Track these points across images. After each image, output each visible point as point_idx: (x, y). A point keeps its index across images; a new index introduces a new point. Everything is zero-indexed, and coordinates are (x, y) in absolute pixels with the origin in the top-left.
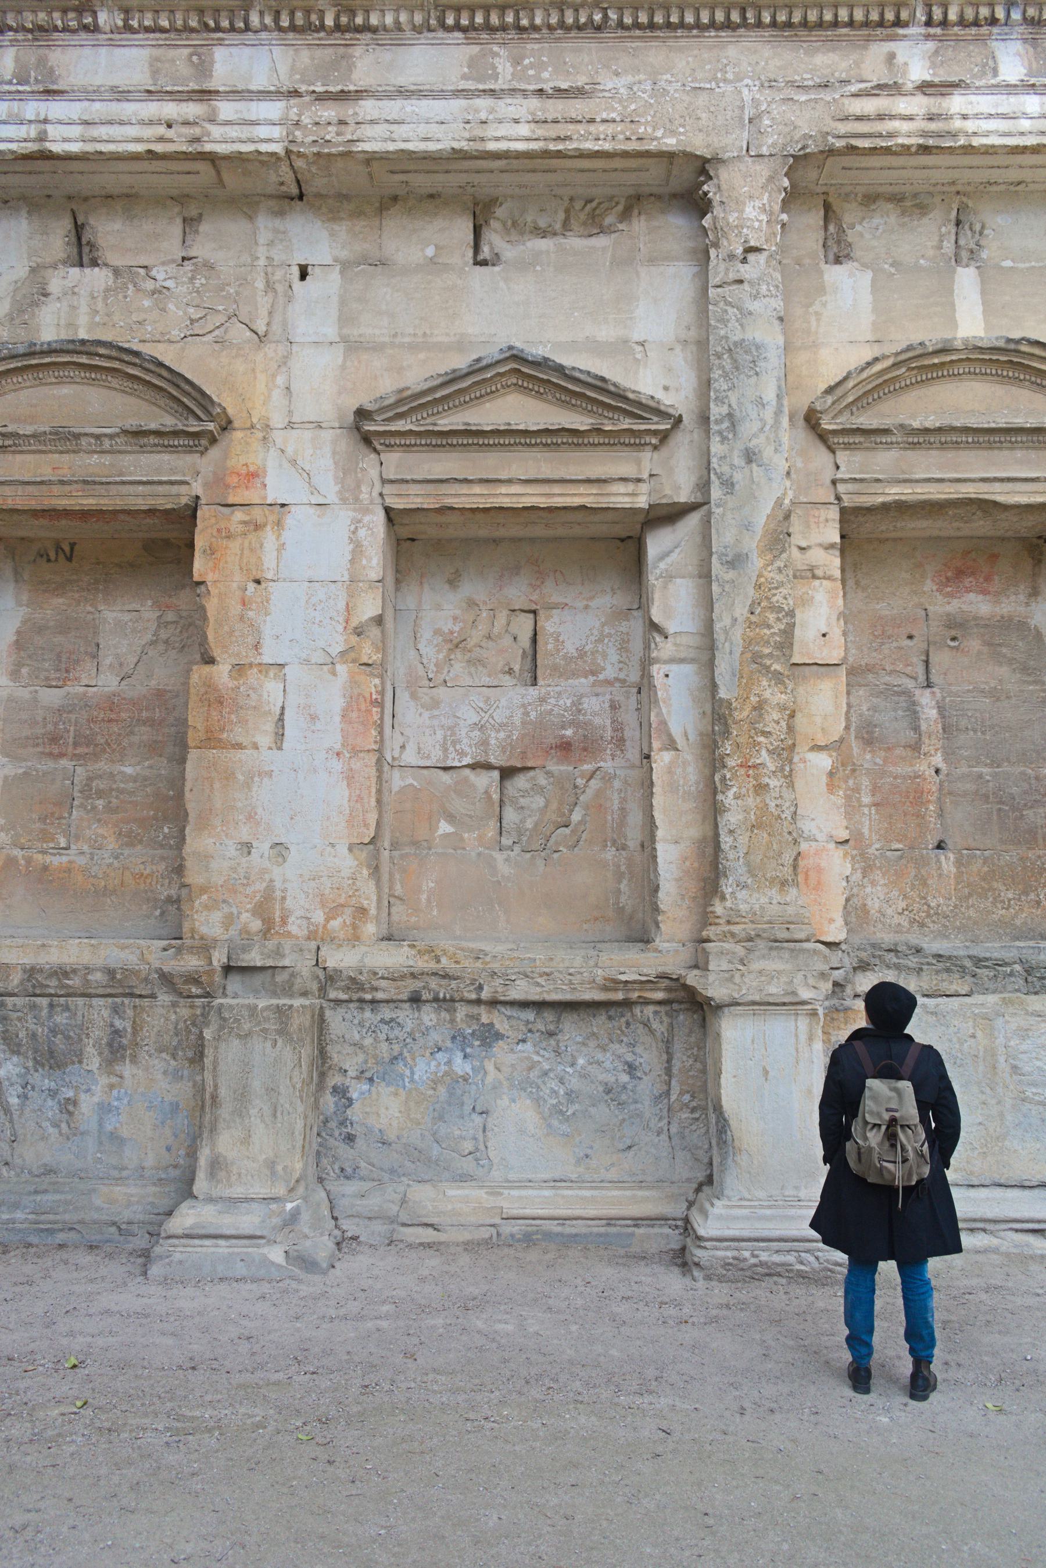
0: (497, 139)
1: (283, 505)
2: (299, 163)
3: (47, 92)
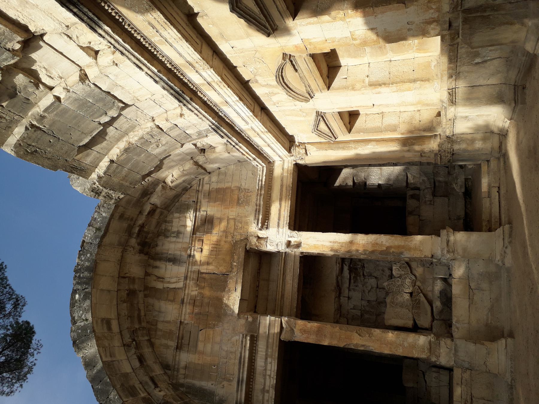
0: (177, 35)
1: (302, 39)
2: (211, 63)
3: (227, 103)
